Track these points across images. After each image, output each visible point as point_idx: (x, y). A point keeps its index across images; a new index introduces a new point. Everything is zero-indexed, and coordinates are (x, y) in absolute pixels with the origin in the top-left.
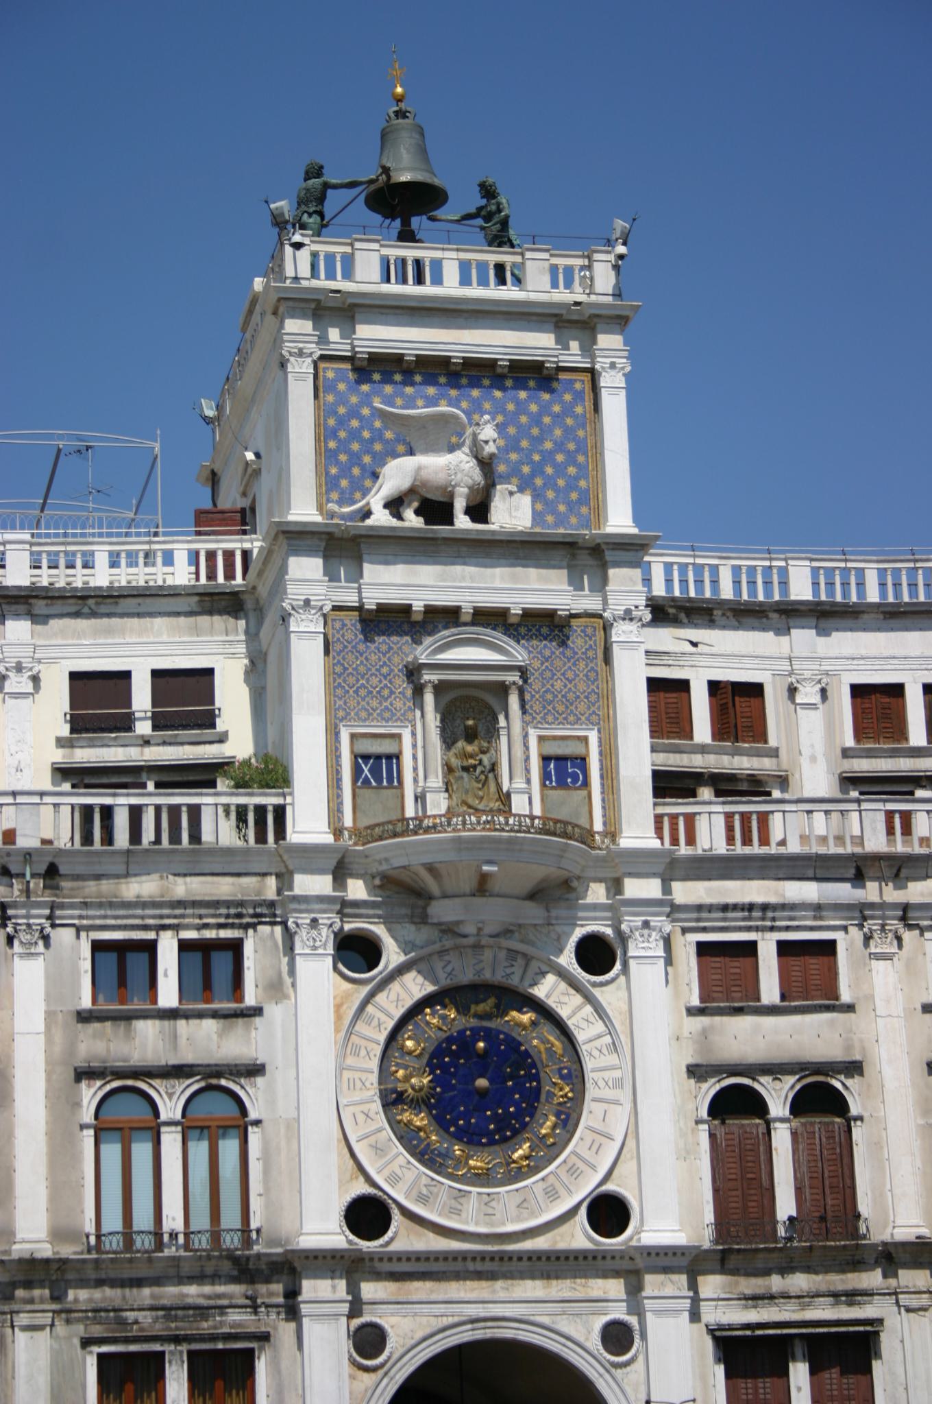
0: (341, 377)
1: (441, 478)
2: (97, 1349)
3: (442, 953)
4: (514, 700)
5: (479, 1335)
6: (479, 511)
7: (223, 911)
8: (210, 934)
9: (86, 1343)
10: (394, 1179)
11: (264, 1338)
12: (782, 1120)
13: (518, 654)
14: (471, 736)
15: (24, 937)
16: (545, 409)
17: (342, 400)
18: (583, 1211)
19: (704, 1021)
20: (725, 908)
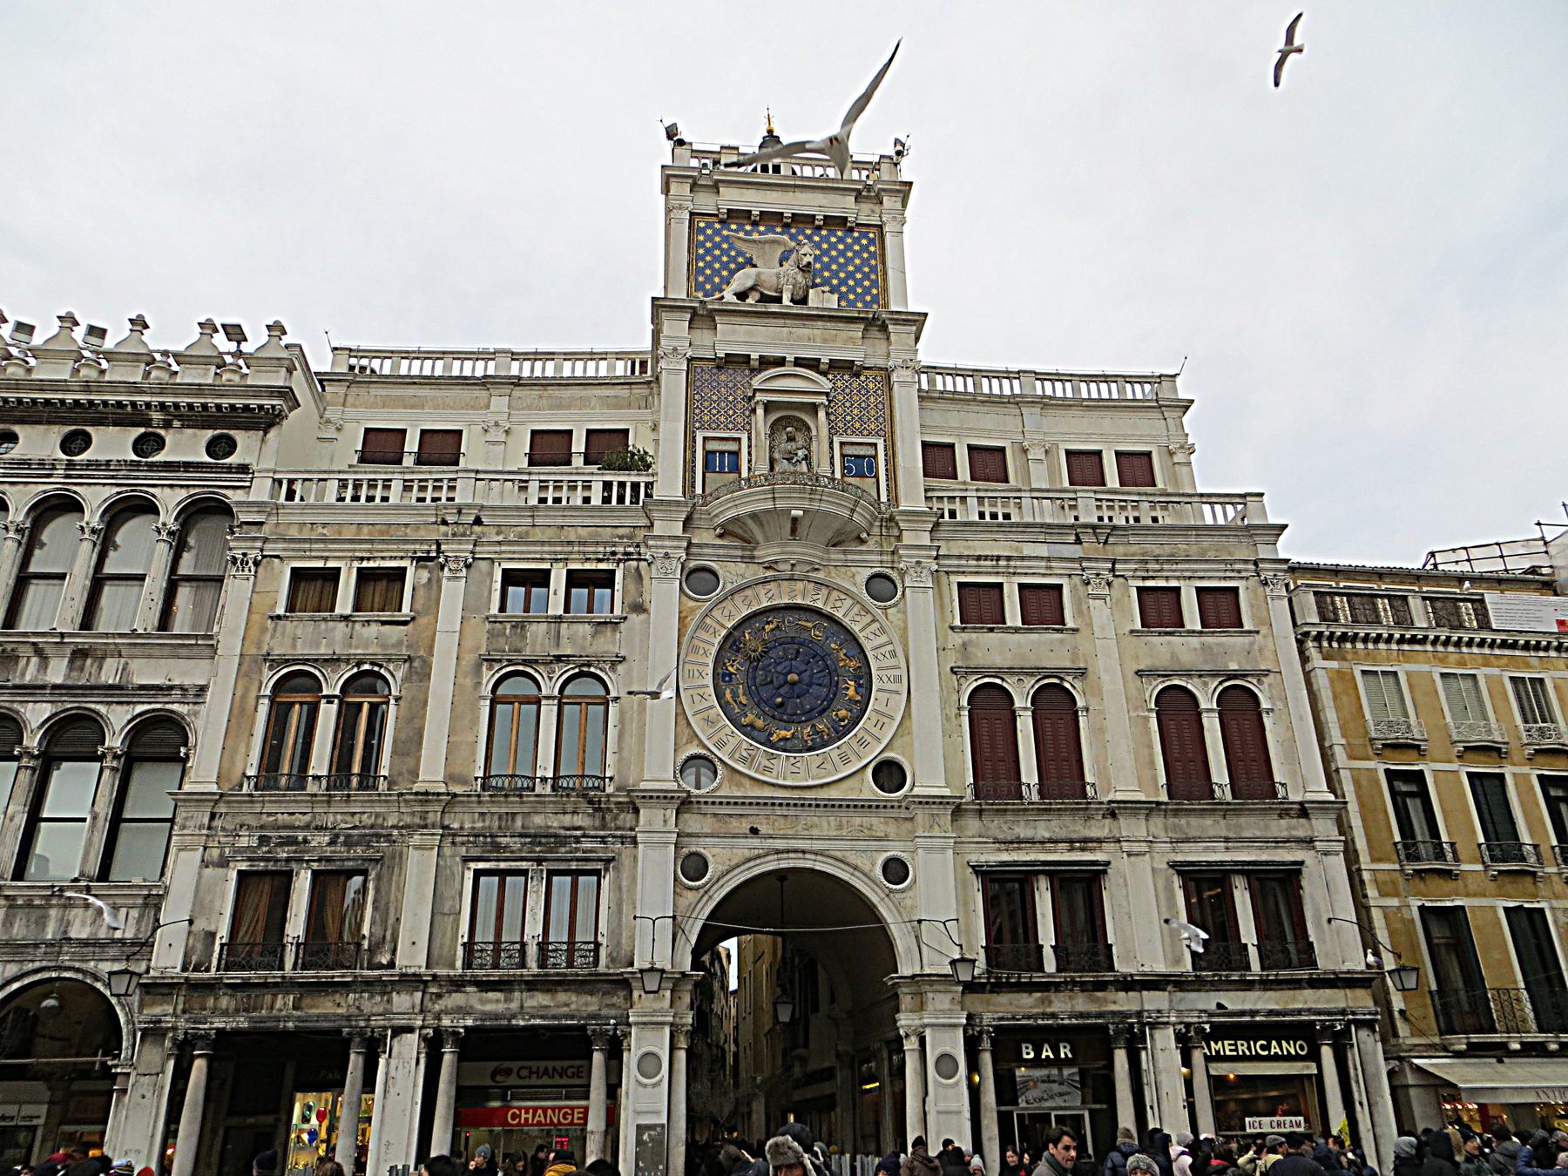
0: (709, 225)
1: (774, 280)
2: (473, 865)
3: (765, 582)
4: (822, 414)
5: (784, 865)
7: (601, 549)
8: (588, 566)
9: (466, 860)
10: (721, 744)
11: (608, 861)
12: (1026, 709)
13: (825, 384)
14: (791, 439)
15: (453, 566)
16: (848, 247)
18: (870, 771)
19: (965, 636)
20: (979, 558)
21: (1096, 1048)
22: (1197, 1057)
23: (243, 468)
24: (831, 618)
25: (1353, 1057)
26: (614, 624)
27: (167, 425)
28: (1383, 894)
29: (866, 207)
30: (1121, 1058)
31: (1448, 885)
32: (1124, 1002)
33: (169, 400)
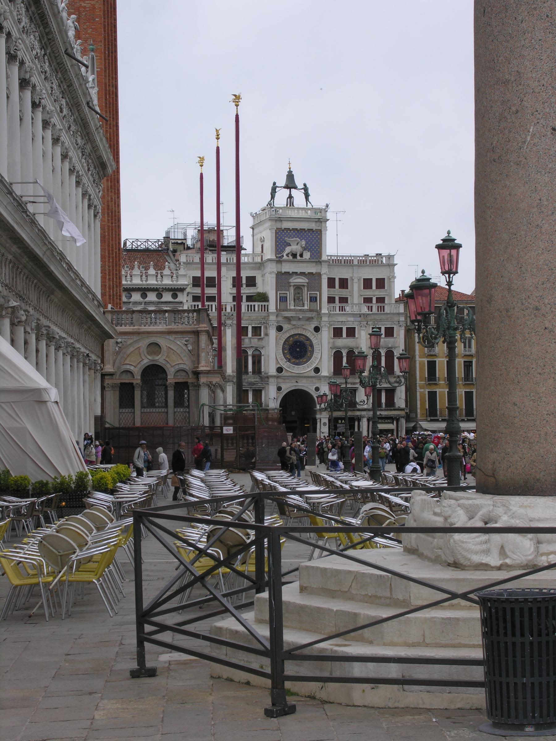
0: (280, 231)
3: (293, 329)
6: (301, 256)
14: (299, 293)
16: (313, 236)
17: (279, 236)
21: (352, 421)
22: (371, 423)
23: (181, 303)
24: (306, 336)
25: (400, 423)
26: (262, 339)
27: (162, 291)
28: (421, 388)
29: (318, 224)
30: (356, 423)
31: (435, 387)
32: (358, 413)
33: (164, 287)
